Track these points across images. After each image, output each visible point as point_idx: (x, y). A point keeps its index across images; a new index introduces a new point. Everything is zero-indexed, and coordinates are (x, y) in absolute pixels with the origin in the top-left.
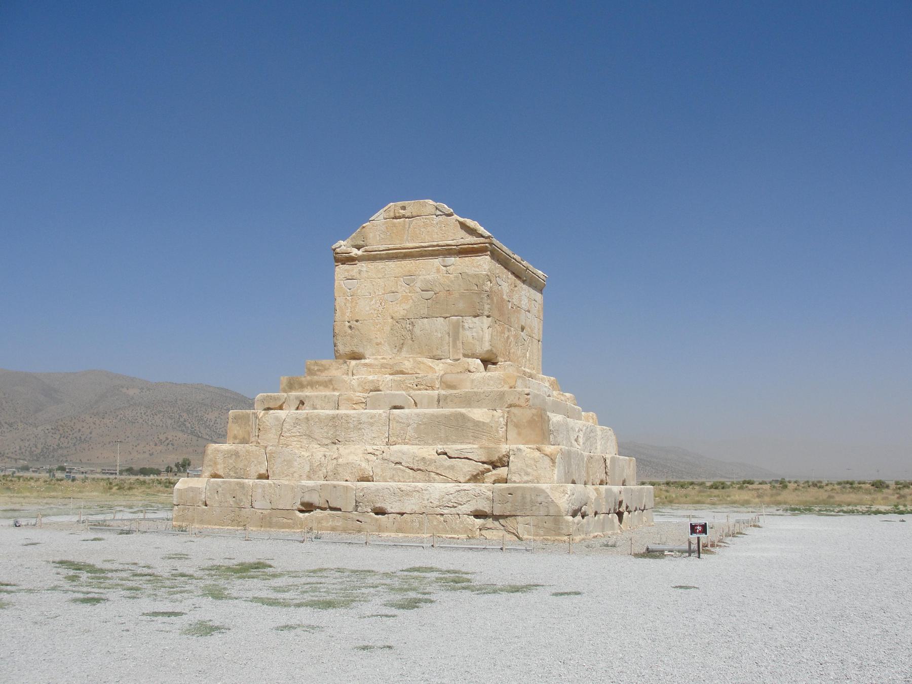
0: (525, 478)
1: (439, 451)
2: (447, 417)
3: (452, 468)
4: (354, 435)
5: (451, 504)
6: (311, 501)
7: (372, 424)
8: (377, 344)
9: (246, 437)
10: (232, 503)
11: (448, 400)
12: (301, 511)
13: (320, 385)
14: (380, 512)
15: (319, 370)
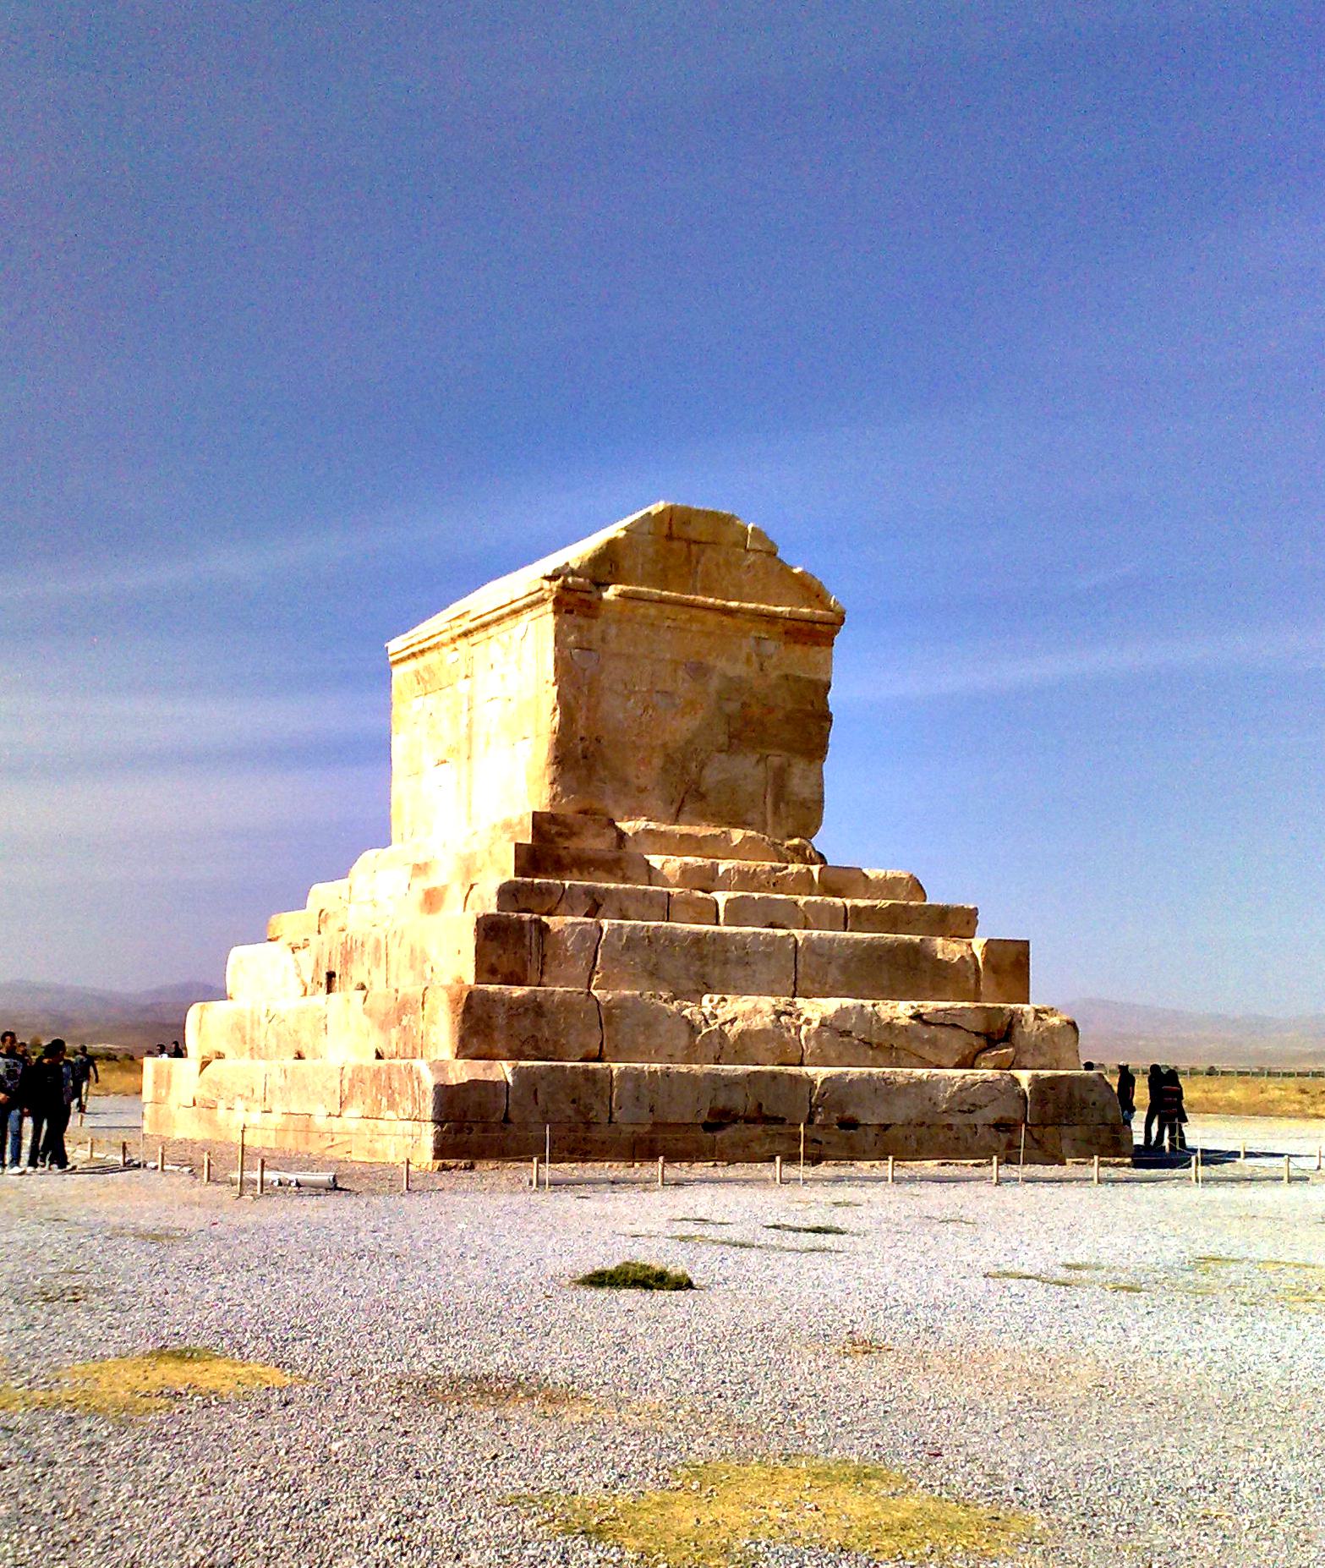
0: (1041, 1060)
1: (911, 1012)
2: (892, 950)
3: (933, 1042)
4: (738, 973)
5: (966, 1108)
6: (730, 1105)
7: (768, 955)
8: (641, 790)
9: (518, 969)
10: (570, 1112)
11: (863, 917)
12: (708, 1127)
13: (597, 869)
14: (849, 1124)
15: (560, 834)
